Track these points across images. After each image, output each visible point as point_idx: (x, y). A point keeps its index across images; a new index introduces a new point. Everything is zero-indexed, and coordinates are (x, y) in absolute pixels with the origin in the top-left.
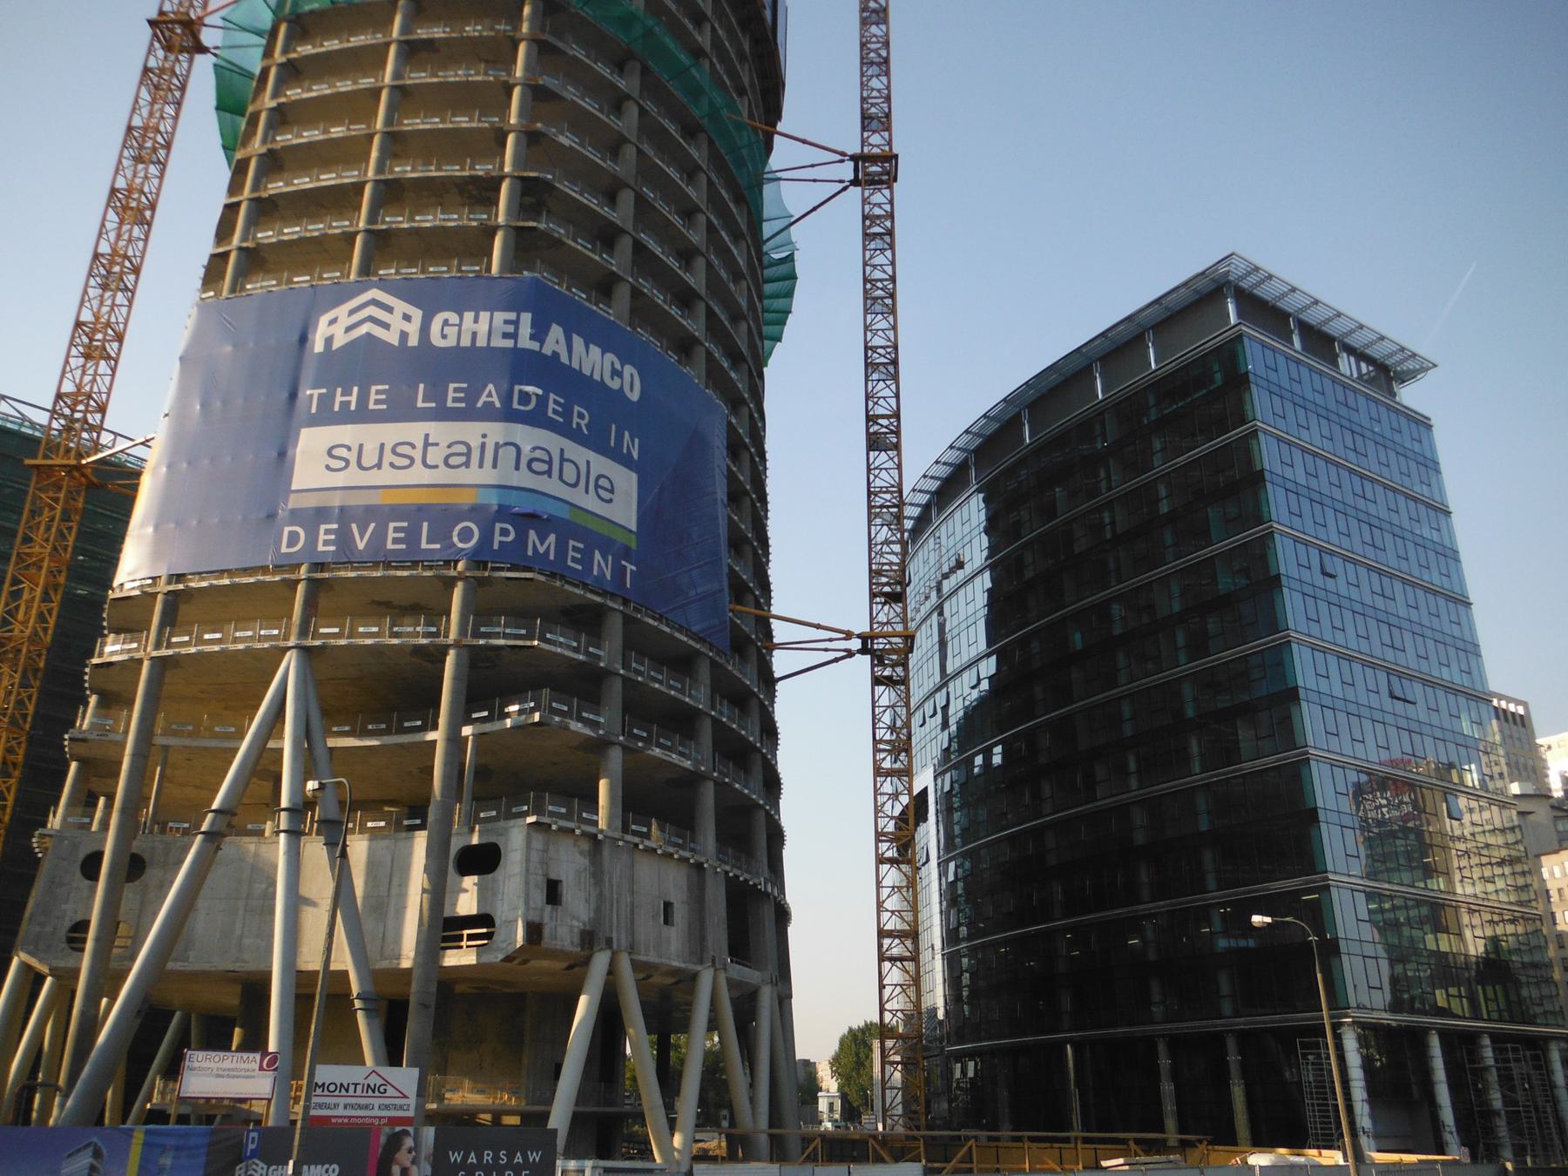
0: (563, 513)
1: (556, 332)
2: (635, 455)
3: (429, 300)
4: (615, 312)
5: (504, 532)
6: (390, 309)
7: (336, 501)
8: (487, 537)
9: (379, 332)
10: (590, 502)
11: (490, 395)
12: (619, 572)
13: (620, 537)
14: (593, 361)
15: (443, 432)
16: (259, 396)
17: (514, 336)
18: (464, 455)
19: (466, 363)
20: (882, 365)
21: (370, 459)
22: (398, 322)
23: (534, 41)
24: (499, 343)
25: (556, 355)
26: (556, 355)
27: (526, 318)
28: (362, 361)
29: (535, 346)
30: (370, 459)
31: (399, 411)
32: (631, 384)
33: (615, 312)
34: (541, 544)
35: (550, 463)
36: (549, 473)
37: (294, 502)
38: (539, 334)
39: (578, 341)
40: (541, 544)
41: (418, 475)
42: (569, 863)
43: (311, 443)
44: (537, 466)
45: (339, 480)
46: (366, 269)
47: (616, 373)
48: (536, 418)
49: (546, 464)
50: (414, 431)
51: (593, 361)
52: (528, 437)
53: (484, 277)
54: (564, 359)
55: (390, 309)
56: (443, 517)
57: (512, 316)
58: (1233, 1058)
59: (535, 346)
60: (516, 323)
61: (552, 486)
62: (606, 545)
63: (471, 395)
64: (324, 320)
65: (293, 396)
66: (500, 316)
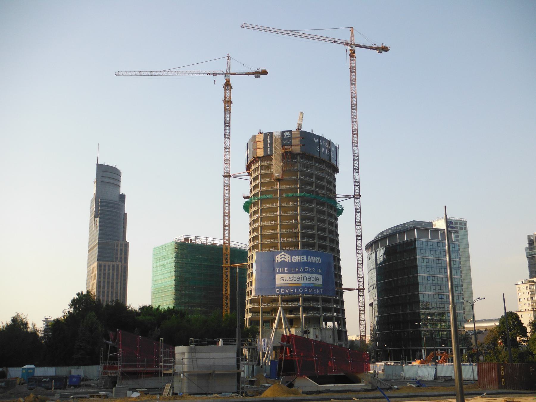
0: (313, 285)
1: (309, 257)
3: (292, 254)
4: (316, 250)
7: (283, 286)
8: (304, 290)
9: (285, 259)
10: (316, 282)
11: (302, 269)
12: (320, 291)
13: (320, 286)
15: (296, 275)
16: (270, 269)
17: (303, 260)
18: (299, 279)
19: (298, 264)
20: (358, 224)
21: (287, 279)
22: (287, 258)
23: (301, 206)
24: (302, 261)
28: (283, 264)
30: (287, 279)
31: (289, 272)
33: (316, 250)
34: (310, 291)
37: (277, 286)
38: (307, 259)
41: (293, 282)
42: (318, 332)
43: (278, 276)
45: (283, 282)
46: (281, 249)
48: (308, 272)
49: (310, 279)
50: (292, 275)
51: (314, 259)
52: (307, 275)
53: (298, 250)
56: (297, 288)
58: (411, 353)
61: (311, 282)
62: (318, 288)
63: (299, 269)
64: (276, 257)
65: (274, 269)
66: (302, 256)
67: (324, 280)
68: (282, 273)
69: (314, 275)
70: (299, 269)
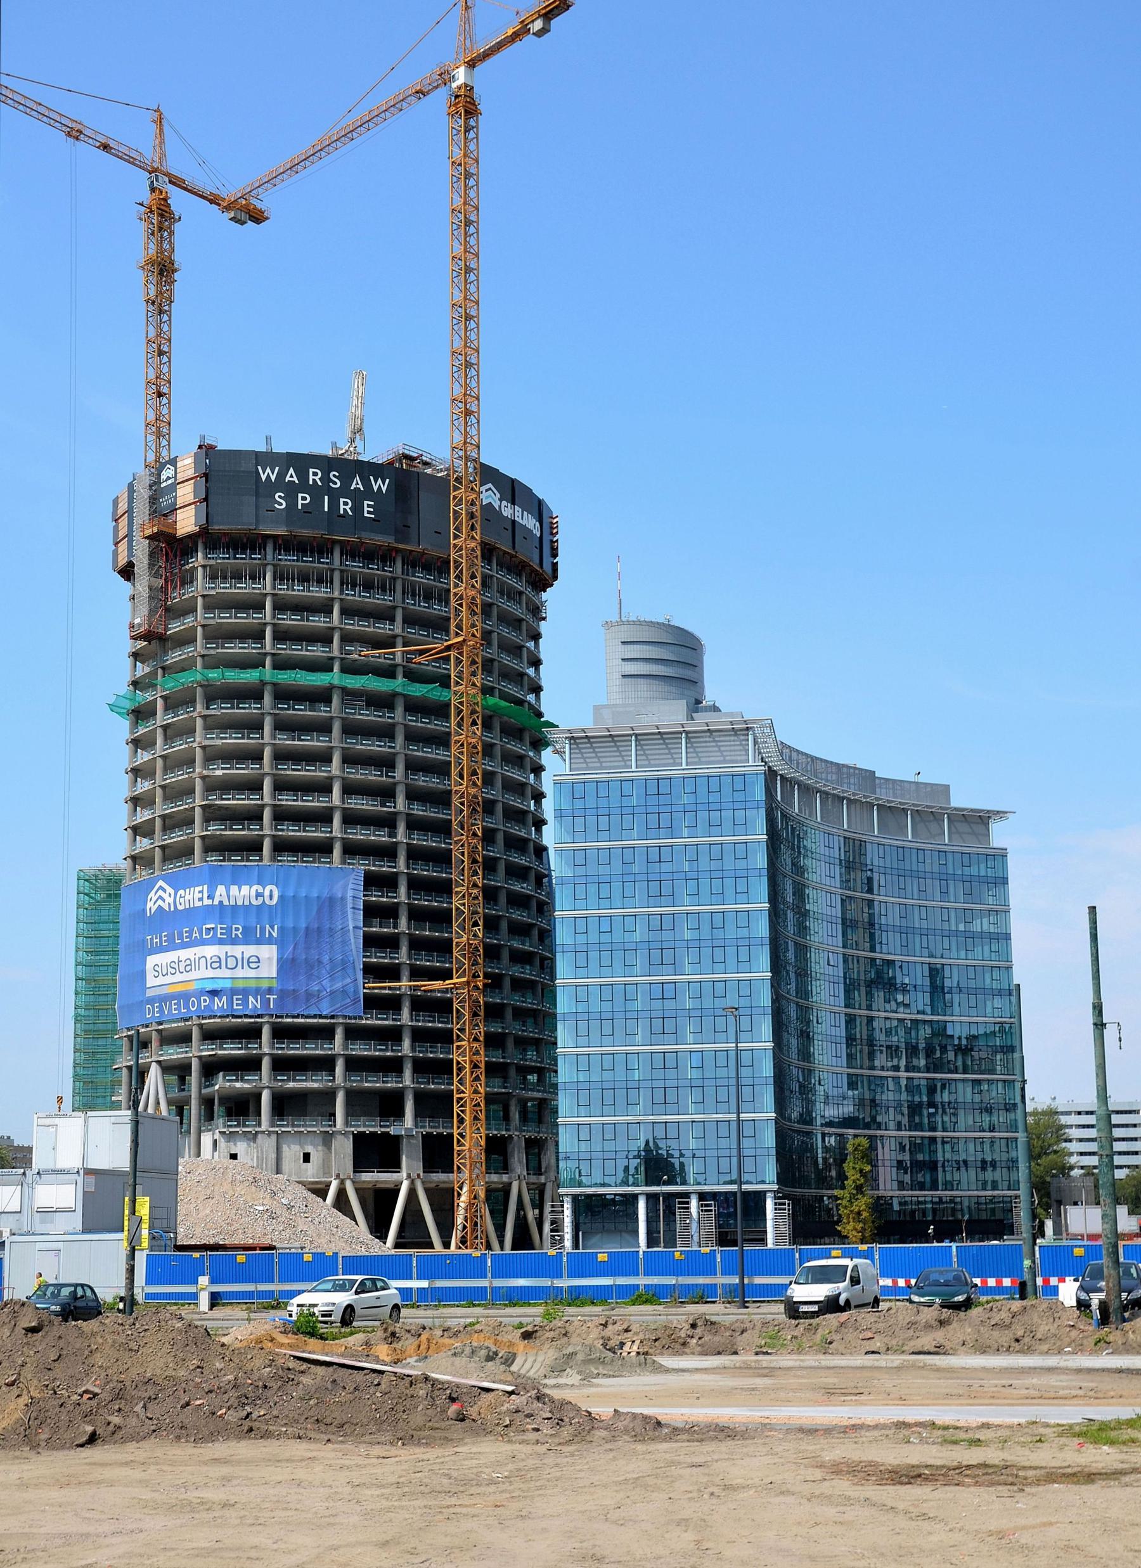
0: (228, 984)
1: (221, 889)
2: (275, 935)
5: (205, 1001)
6: (165, 891)
13: (265, 985)
14: (244, 894)
25: (221, 902)
26: (221, 902)
27: (206, 887)
29: (210, 902)
32: (271, 893)
34: (220, 1003)
35: (220, 962)
36: (220, 967)
39: (234, 889)
40: (220, 1003)
44: (215, 965)
47: (258, 895)
49: (218, 962)
51: (244, 894)
54: (226, 903)
55: (165, 891)
57: (200, 888)
59: (210, 902)
60: (201, 892)
61: (224, 973)
67: (286, 966)
68: (161, 950)
69: (237, 950)
70: (191, 932)
